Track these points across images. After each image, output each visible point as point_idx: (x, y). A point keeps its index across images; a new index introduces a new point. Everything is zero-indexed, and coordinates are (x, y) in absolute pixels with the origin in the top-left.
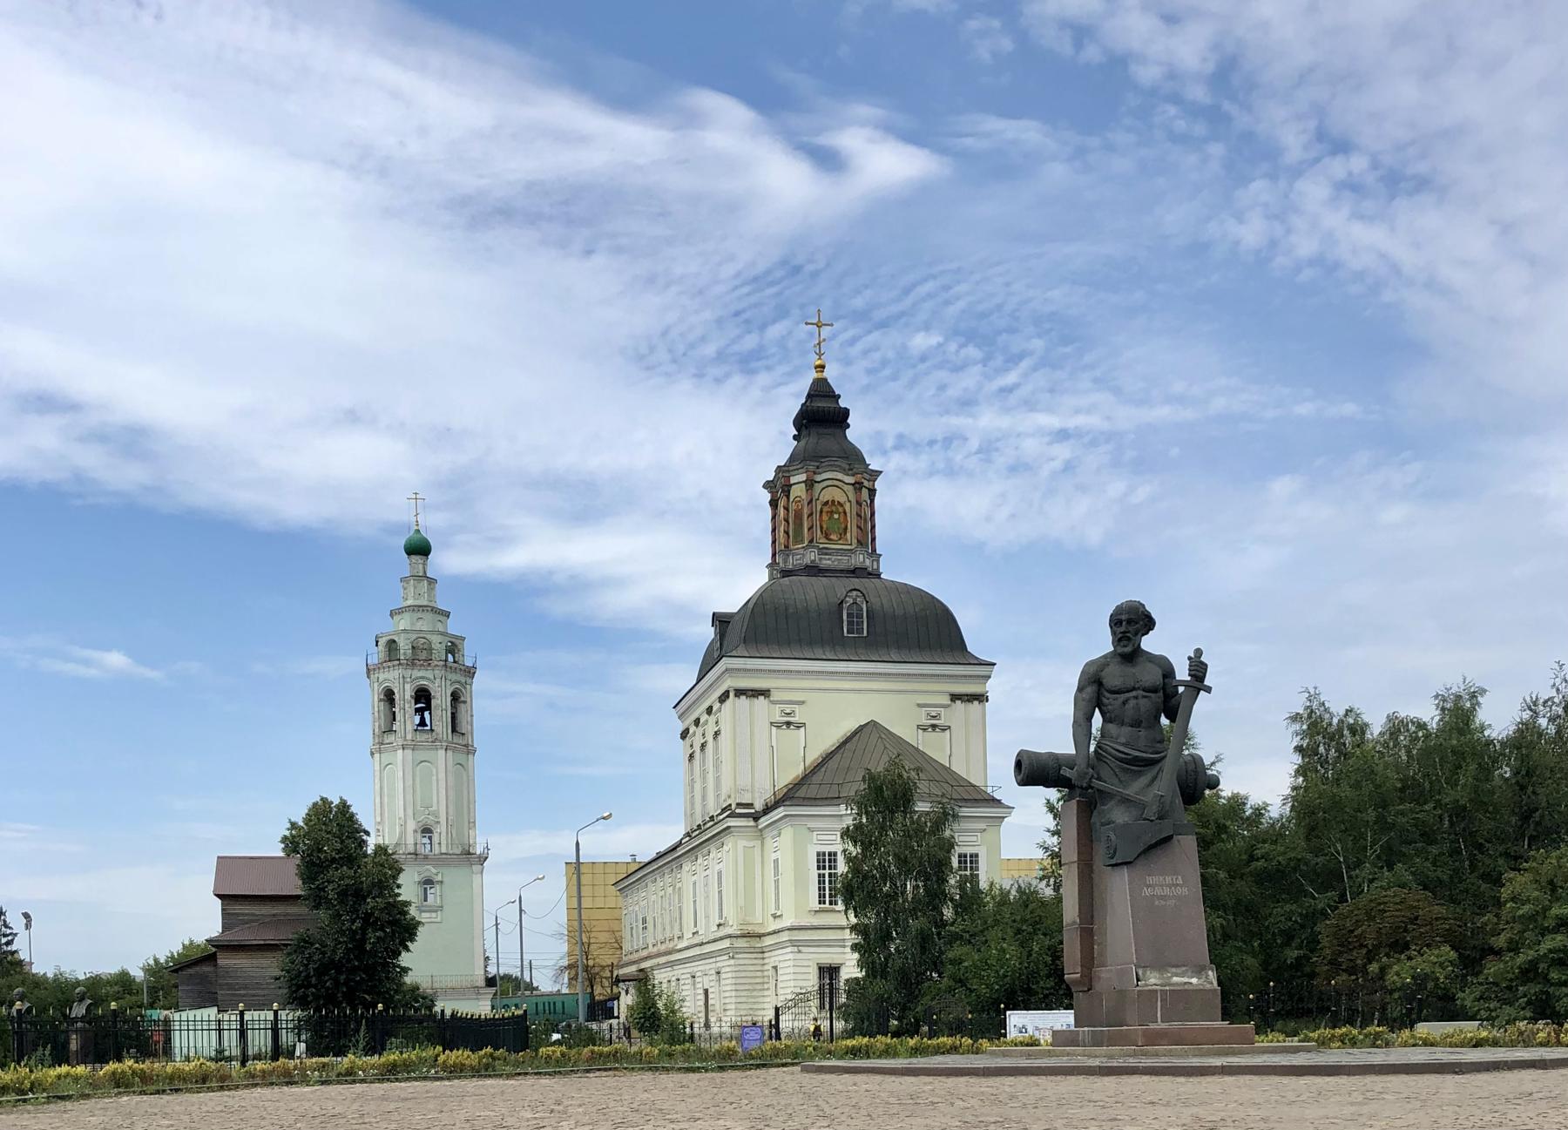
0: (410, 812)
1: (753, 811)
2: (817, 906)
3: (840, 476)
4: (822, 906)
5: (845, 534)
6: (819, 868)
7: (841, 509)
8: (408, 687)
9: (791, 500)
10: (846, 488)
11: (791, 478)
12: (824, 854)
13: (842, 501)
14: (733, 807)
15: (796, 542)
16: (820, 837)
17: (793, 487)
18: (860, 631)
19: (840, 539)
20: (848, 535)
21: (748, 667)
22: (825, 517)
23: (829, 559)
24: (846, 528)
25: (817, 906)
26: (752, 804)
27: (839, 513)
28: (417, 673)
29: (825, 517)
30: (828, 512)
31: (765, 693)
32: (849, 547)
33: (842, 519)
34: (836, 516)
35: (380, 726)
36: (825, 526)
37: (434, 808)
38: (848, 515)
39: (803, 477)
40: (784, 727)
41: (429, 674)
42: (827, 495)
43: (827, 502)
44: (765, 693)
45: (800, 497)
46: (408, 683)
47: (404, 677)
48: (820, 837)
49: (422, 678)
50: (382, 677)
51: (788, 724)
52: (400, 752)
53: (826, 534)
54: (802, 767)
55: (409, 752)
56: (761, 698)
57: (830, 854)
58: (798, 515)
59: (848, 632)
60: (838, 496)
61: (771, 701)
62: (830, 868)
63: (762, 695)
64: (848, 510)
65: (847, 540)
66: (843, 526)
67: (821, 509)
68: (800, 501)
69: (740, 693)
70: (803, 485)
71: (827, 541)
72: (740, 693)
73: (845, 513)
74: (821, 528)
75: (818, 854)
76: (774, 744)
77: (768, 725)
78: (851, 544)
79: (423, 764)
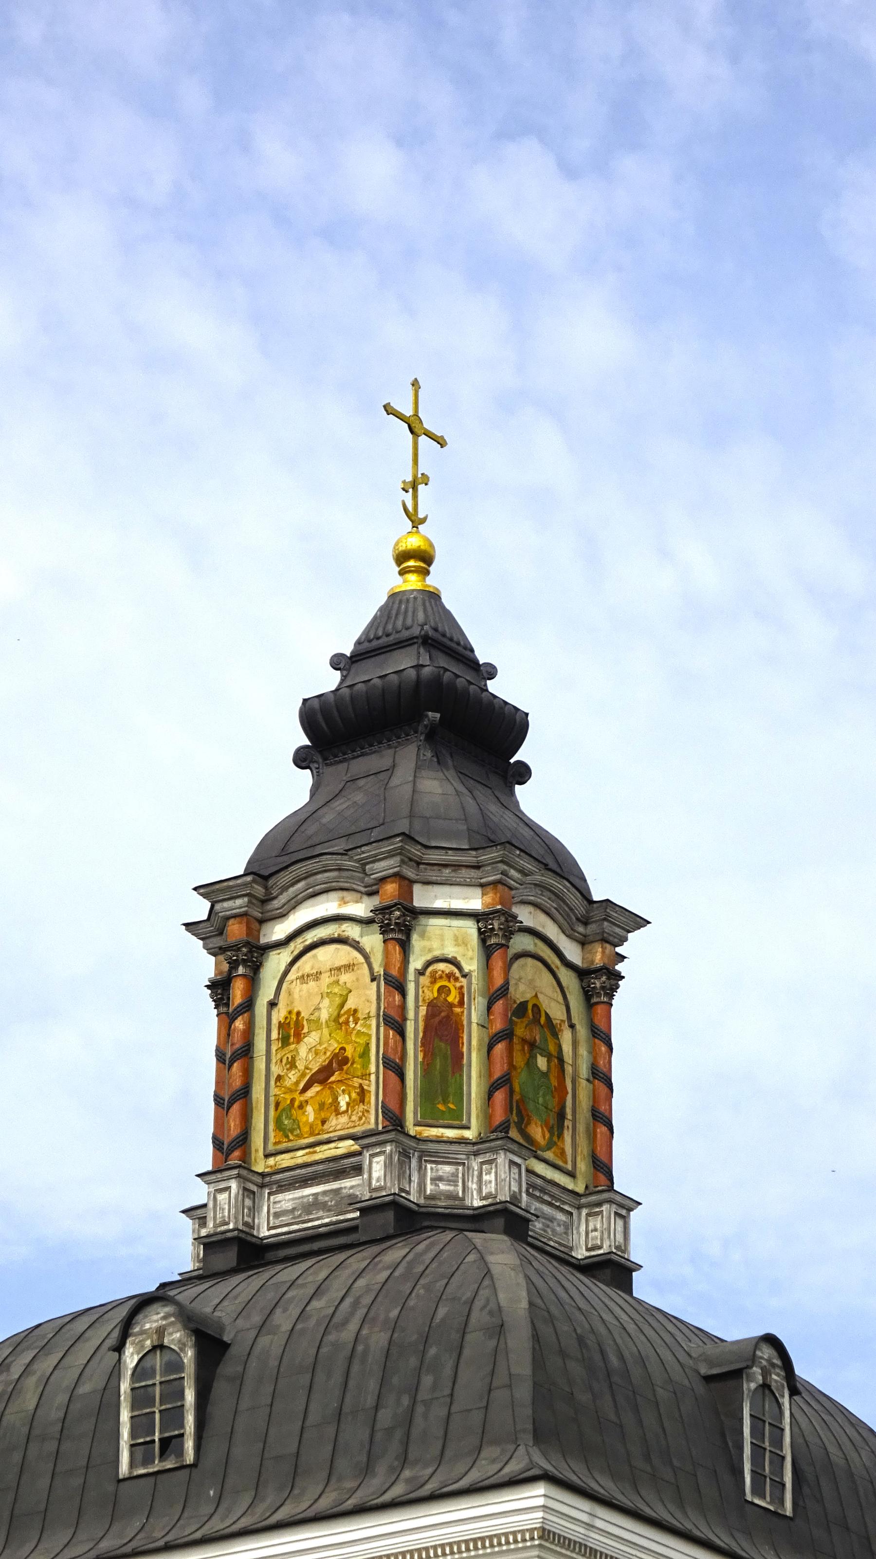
3: (551, 931)
9: (416, 963)
11: (417, 889)
13: (557, 1013)
17: (423, 920)
19: (548, 1148)
24: (561, 1116)
27: (549, 1057)
30: (524, 1041)
32: (570, 1186)
34: (542, 1063)
39: (475, 902)
64: (567, 1048)
65: (563, 1153)
66: (553, 1103)
68: (450, 976)
70: (470, 928)
73: (561, 1061)
78: (572, 1175)
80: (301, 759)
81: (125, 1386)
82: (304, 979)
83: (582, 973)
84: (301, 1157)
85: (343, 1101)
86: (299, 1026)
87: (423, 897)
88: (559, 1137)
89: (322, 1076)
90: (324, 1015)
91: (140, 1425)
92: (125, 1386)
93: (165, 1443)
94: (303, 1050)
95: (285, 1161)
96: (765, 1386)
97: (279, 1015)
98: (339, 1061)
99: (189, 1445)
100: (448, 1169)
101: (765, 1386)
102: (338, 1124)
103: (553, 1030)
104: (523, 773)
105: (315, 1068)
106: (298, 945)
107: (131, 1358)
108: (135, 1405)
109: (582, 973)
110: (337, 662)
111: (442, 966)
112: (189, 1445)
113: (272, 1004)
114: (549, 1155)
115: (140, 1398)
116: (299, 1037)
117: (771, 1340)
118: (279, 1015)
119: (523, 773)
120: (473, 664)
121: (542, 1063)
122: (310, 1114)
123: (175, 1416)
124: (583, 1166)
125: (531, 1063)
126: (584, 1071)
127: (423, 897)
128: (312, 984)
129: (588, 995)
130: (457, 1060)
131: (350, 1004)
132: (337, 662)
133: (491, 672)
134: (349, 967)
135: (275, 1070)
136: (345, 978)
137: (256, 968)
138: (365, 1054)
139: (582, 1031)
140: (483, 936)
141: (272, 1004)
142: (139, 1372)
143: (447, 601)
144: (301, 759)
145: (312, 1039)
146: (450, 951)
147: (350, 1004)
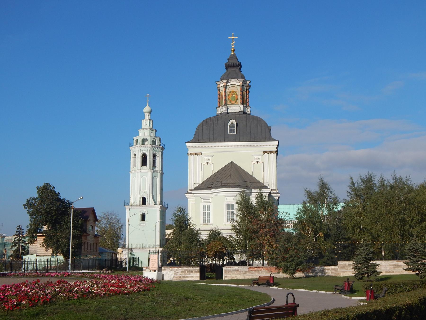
2: (202, 223)
4: (205, 223)
5: (237, 101)
6: (204, 211)
7: (235, 94)
8: (139, 153)
10: (237, 87)
12: (205, 206)
13: (236, 91)
16: (204, 200)
18: (234, 132)
19: (235, 103)
20: (238, 101)
21: (194, 146)
22: (230, 96)
23: (232, 109)
24: (237, 100)
25: (202, 223)
29: (230, 96)
30: (231, 95)
31: (201, 154)
32: (238, 105)
33: (236, 97)
34: (234, 96)
36: (230, 100)
37: (146, 191)
38: (238, 95)
40: (206, 164)
42: (231, 90)
43: (231, 92)
44: (201, 154)
48: (204, 200)
53: (231, 101)
56: (199, 155)
57: (207, 206)
59: (230, 133)
60: (235, 89)
62: (207, 211)
63: (199, 154)
64: (238, 93)
65: (237, 103)
67: (229, 94)
71: (231, 104)
73: (237, 94)
74: (229, 100)
75: (204, 206)
77: (200, 163)
79: (142, 177)
88: (237, 101)
96: (232, 123)
101: (232, 123)
111: (222, 91)
114: (235, 104)
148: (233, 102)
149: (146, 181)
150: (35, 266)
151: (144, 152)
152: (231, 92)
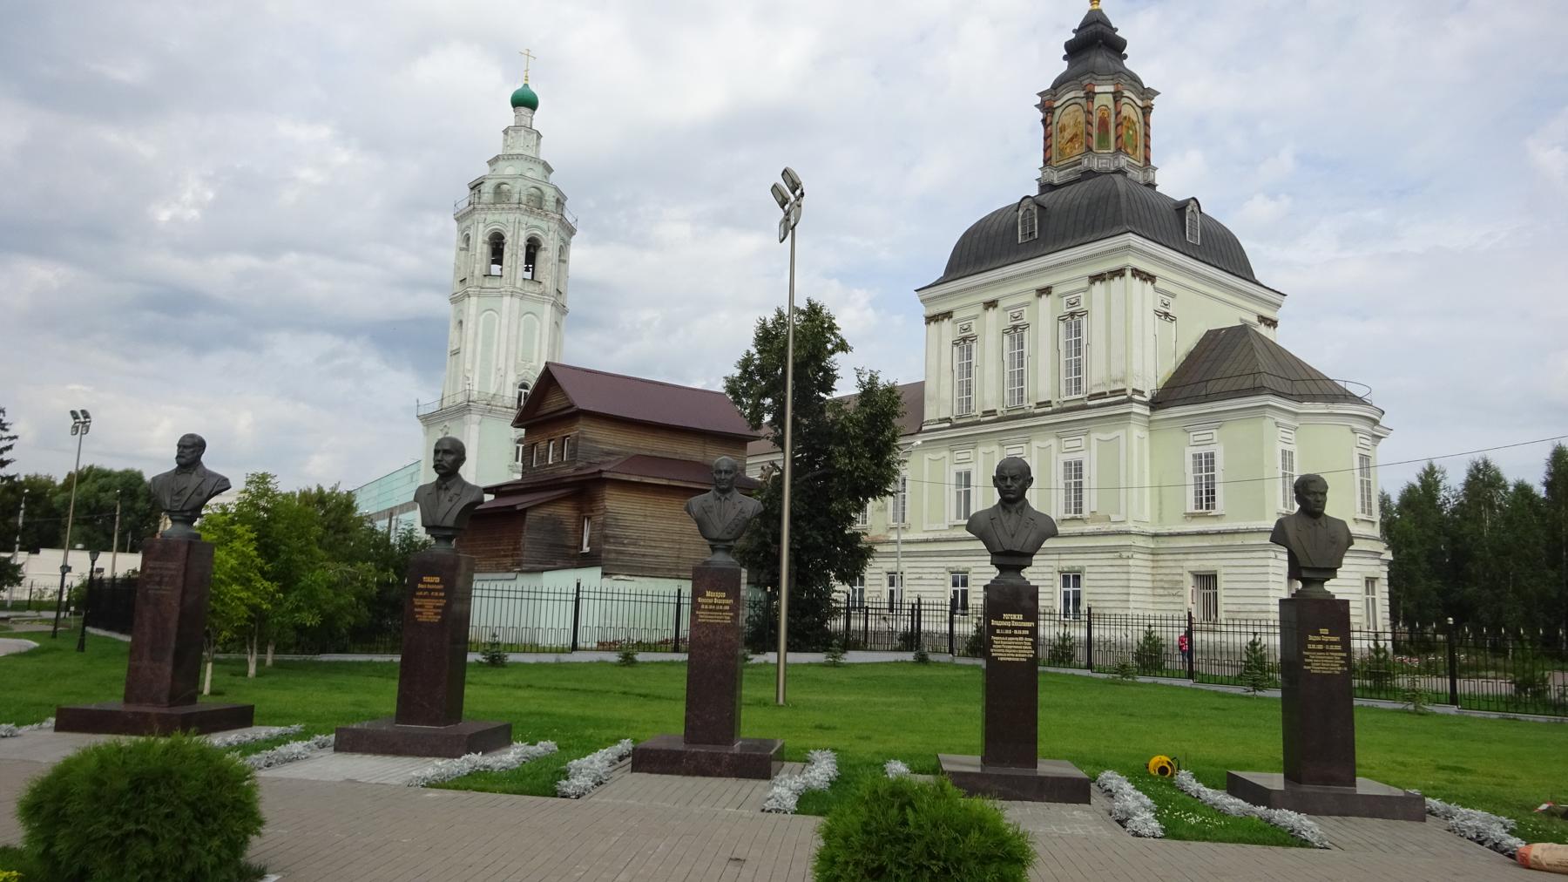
0: (511, 363)
1: (1144, 399)
3: (1133, 97)
9: (1096, 107)
10: (1137, 109)
11: (1096, 87)
13: (1135, 119)
14: (1129, 392)
15: (1100, 146)
17: (1097, 95)
19: (1134, 154)
21: (1145, 248)
24: (1136, 147)
26: (1143, 392)
28: (532, 221)
34: (1131, 132)
35: (481, 270)
39: (1111, 89)
40: (1163, 317)
41: (544, 225)
45: (1106, 106)
46: (522, 228)
47: (519, 223)
49: (536, 227)
50: (490, 218)
51: (1167, 314)
52: (507, 300)
54: (1174, 362)
55: (516, 301)
58: (1103, 123)
61: (1155, 288)
64: (1138, 130)
66: (1134, 143)
69: (1136, 273)
70: (1111, 96)
72: (1136, 273)
76: (1157, 333)
78: (1139, 162)
80: (1065, 58)
81: (1019, 220)
82: (1066, 115)
83: (1142, 108)
84: (1066, 162)
85: (1077, 146)
86: (1064, 128)
87: (1097, 89)
89: (1071, 140)
90: (1072, 123)
91: (1024, 229)
92: (1019, 220)
93: (1030, 233)
94: (1066, 133)
95: (1061, 163)
96: (1193, 211)
97: (1060, 125)
98: (1076, 135)
99: (1036, 234)
100: (1104, 161)
101: (1193, 211)
102: (1075, 152)
103: (1134, 124)
104: (1125, 56)
105: (1069, 137)
106: (1064, 106)
107: (1021, 213)
108: (1022, 224)
109: (1142, 108)
110: (1074, 31)
112: (1036, 234)
113: (1057, 123)
115: (1023, 222)
116: (1065, 130)
117: (1194, 199)
118: (1060, 125)
119: (1125, 56)
120: (1111, 28)
121: (1131, 132)
122: (1068, 150)
123: (1032, 226)
124: (1142, 160)
125: (1128, 132)
126: (1142, 134)
127: (1097, 89)
128: (1068, 116)
129: (1144, 114)
130: (1107, 132)
131: (1079, 120)
132: (1074, 31)
133: (1117, 30)
134: (1078, 110)
135: (1059, 140)
136: (1077, 113)
137: (1053, 113)
138: (1082, 133)
139: (1142, 123)
140: (1114, 98)
141: (1057, 123)
142: (1023, 216)
143: (1104, 11)
144: (1065, 58)
145: (1068, 130)
146: (1105, 103)
147: (1079, 120)
148: (1129, 151)
149: (537, 332)
150: (915, 624)
151: (536, 234)
152: (1125, 118)
